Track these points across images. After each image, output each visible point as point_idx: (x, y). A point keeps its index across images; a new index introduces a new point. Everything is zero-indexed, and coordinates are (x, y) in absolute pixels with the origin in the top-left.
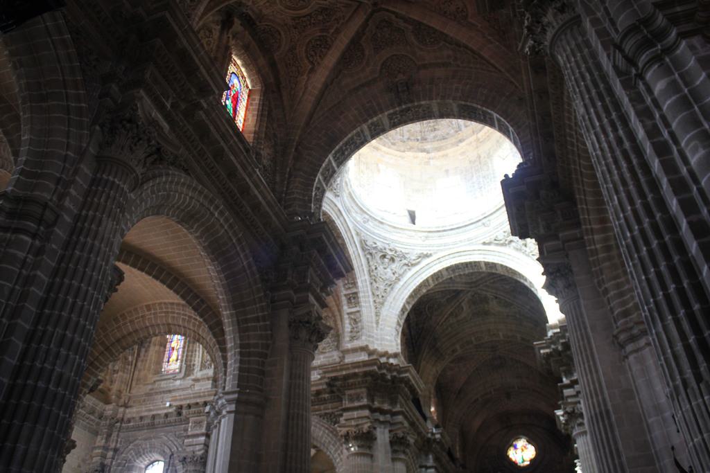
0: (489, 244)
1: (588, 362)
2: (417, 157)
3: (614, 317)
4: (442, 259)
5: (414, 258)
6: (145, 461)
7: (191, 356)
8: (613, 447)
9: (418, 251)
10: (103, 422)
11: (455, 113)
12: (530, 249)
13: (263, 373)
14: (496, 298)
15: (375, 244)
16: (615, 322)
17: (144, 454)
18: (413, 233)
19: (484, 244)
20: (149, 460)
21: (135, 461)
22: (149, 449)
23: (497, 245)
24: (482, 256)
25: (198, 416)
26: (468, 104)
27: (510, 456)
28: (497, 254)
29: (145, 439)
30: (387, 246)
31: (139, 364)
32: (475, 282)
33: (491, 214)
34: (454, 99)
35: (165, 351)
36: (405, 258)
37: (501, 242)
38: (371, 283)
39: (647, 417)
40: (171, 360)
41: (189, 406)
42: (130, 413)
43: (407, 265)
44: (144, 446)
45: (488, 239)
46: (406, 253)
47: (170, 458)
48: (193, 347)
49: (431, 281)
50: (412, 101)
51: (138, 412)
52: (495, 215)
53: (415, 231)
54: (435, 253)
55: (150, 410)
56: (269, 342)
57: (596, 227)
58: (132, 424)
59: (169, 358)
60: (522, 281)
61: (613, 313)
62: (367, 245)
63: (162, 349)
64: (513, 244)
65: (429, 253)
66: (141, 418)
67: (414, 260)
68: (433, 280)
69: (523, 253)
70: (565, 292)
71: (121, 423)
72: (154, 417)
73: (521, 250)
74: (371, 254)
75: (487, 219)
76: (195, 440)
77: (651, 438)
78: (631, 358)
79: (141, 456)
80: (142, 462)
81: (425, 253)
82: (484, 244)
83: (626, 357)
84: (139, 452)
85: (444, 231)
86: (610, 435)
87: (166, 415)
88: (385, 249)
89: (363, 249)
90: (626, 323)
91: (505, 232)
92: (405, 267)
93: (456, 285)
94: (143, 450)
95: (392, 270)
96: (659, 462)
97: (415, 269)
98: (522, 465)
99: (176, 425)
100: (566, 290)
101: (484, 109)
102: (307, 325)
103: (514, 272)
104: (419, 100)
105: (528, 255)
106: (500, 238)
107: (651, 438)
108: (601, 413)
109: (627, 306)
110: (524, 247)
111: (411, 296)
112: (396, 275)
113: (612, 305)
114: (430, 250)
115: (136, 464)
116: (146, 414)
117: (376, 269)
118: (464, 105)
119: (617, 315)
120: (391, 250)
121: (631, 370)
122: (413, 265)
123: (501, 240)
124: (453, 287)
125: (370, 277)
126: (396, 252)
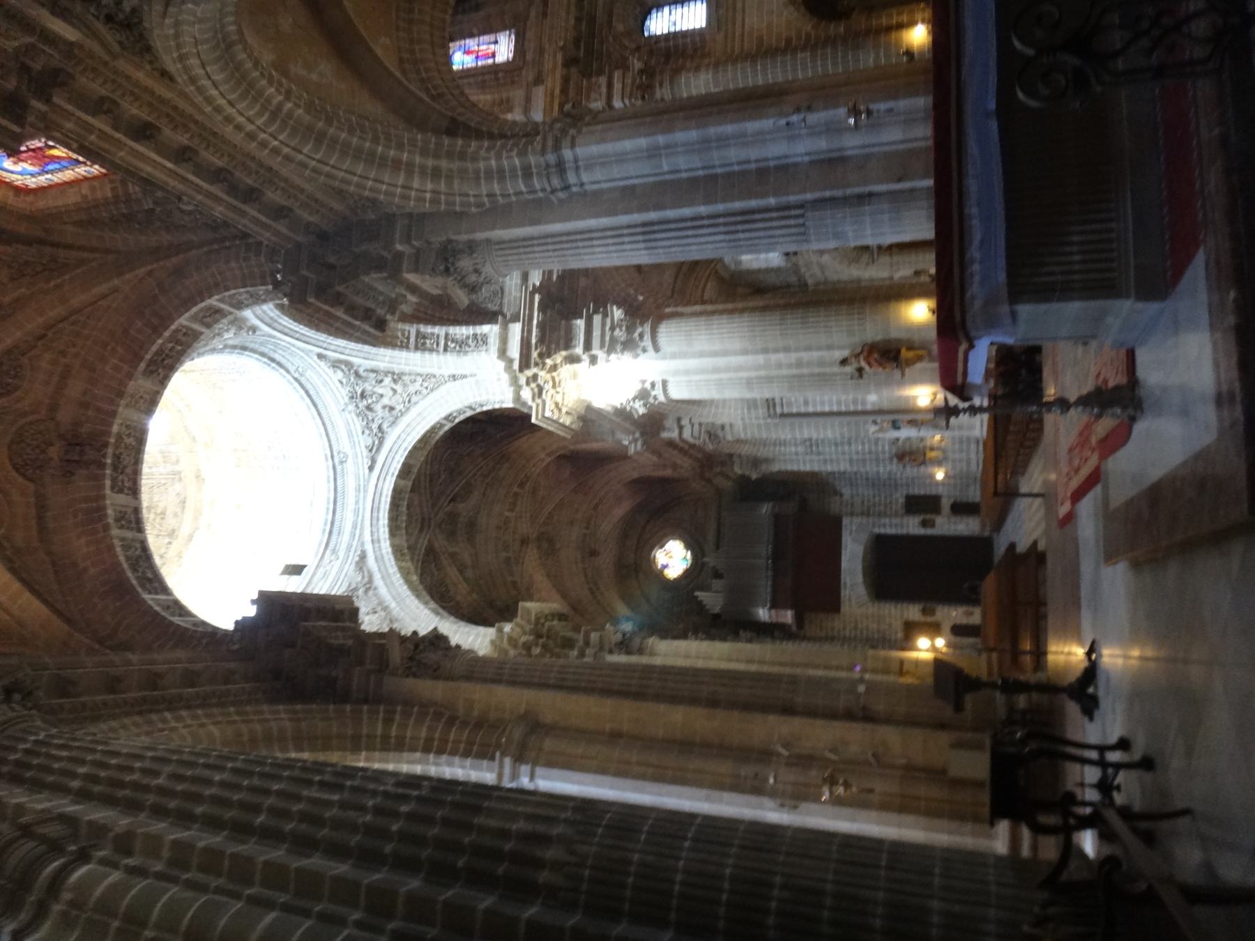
0: (373, 461)
1: (576, 241)
3: (527, 193)
8: (689, 224)
9: (350, 568)
11: (155, 388)
12: (398, 404)
13: (479, 725)
14: (453, 500)
16: (534, 192)
18: (321, 571)
19: (371, 468)
23: (378, 450)
24: (389, 477)
26: (148, 357)
27: (675, 576)
28: (392, 454)
32: (423, 519)
33: (330, 446)
34: (130, 376)
37: (377, 442)
39: (660, 171)
43: (367, 591)
46: (349, 586)
49: (404, 564)
50: (106, 445)
52: (333, 442)
53: (318, 567)
54: (363, 544)
56: (432, 710)
57: (401, 180)
60: (441, 433)
61: (521, 193)
64: (385, 426)
65: (359, 552)
67: (363, 578)
68: (403, 561)
69: (402, 415)
70: (476, 258)
73: (397, 418)
75: (335, 454)
77: (686, 171)
78: (585, 177)
81: (357, 559)
82: (371, 468)
83: (582, 185)
85: (332, 523)
86: (673, 226)
90: (539, 174)
91: (363, 432)
92: (371, 593)
93: (419, 546)
95: (368, 614)
96: (713, 167)
97: (378, 581)
98: (690, 562)
100: (475, 255)
101: (167, 334)
102: (421, 647)
103: (424, 439)
104: (108, 433)
105: (408, 409)
106: (369, 442)
107: (686, 171)
108: (644, 233)
109: (519, 168)
110: (394, 413)
111: (418, 596)
112: (379, 609)
113: (511, 192)
114: (355, 552)
118: (148, 366)
119: (525, 186)
121: (598, 182)
122: (371, 581)
123: (374, 443)
124: (420, 550)
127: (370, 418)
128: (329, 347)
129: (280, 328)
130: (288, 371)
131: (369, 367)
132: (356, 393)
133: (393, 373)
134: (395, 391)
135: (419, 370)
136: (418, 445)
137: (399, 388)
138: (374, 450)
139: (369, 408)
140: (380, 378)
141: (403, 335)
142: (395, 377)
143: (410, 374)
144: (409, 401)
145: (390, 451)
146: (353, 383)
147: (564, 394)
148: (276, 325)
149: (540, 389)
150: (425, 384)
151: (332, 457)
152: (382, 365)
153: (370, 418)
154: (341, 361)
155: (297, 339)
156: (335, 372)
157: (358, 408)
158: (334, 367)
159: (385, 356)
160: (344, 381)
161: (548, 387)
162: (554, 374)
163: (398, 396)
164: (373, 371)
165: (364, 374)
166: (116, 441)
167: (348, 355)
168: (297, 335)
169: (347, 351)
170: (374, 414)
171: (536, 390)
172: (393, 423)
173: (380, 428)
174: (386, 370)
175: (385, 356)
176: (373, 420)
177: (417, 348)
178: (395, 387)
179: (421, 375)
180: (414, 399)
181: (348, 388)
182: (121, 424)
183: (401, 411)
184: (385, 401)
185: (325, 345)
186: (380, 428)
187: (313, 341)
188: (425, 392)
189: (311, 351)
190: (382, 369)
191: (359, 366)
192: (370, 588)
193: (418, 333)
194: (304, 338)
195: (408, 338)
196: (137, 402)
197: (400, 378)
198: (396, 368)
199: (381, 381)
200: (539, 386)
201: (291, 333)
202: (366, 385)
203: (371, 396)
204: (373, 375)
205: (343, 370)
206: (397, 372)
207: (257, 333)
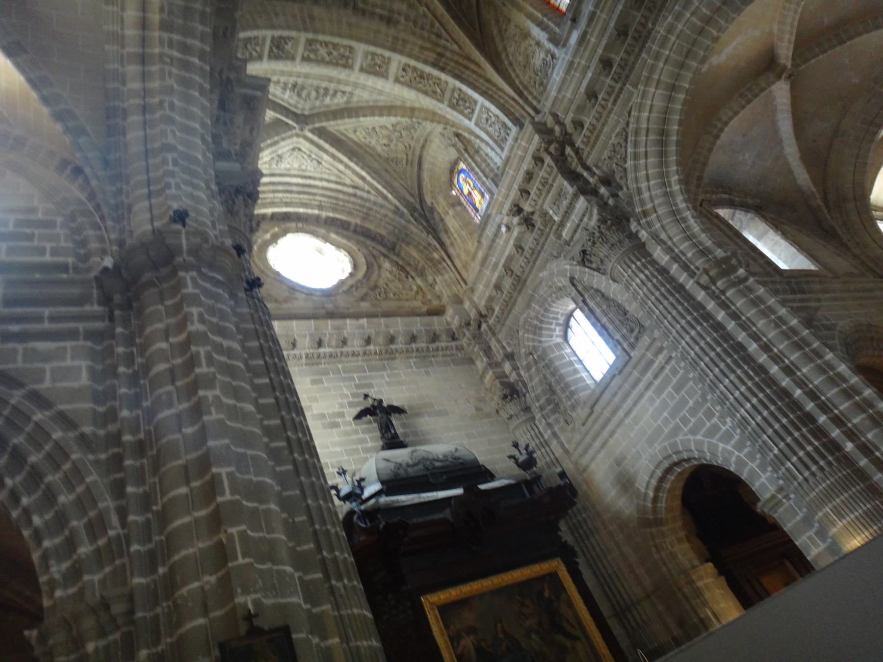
6: (554, 330)
7: (488, 165)
10: (464, 342)
17: (542, 322)
20: (558, 324)
21: (540, 342)
22: (542, 311)
25: (549, 192)
29: (528, 306)
31: (451, 251)
35: (465, 207)
40: (477, 205)
41: (525, 192)
42: (480, 298)
44: (533, 314)
47: (574, 285)
48: (481, 157)
51: (487, 286)
55: (496, 265)
58: (497, 309)
59: (474, 206)
63: (458, 208)
66: (498, 287)
71: (486, 322)
72: (508, 268)
76: (574, 217)
79: (541, 329)
80: (551, 336)
84: (535, 327)
87: (519, 247)
94: (537, 318)
99: (543, 244)
115: (545, 345)
116: (496, 275)
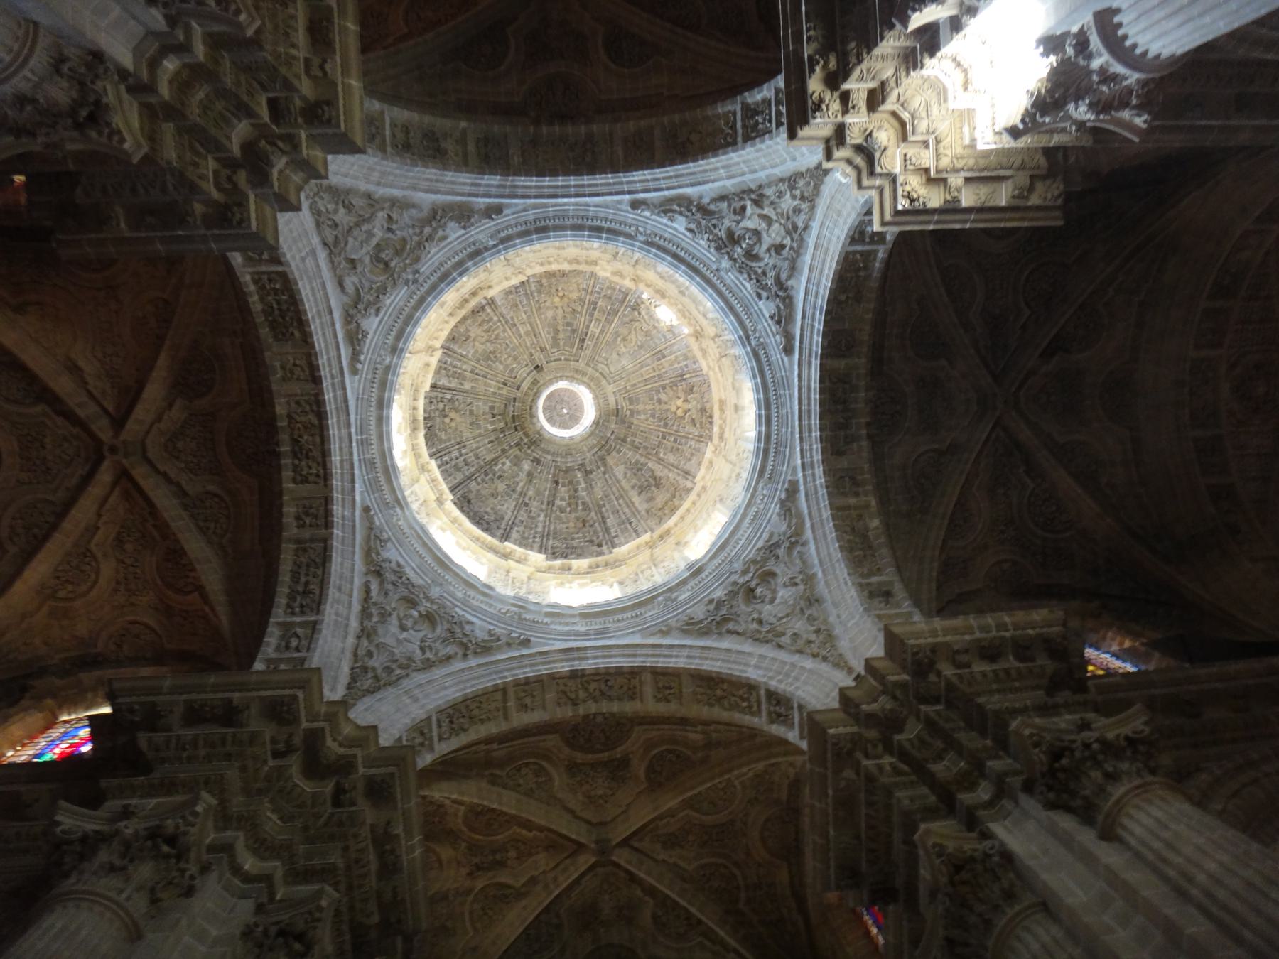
0: (789, 337)
2: (711, 462)
4: (807, 460)
5: (784, 528)
9: (775, 509)
12: (784, 238)
15: (711, 601)
19: (788, 350)
23: (790, 318)
24: (813, 360)
30: (734, 578)
36: (777, 545)
38: (780, 646)
43: (790, 550)
45: (778, 337)
46: (771, 535)
62: (701, 622)
64: (783, 276)
68: (844, 494)
74: (725, 620)
81: (783, 496)
88: (735, 583)
89: (704, 633)
91: (759, 296)
105: (802, 240)
110: (785, 252)
114: (784, 483)
117: (760, 622)
120: (745, 572)
122: (799, 532)
123: (778, 307)
125: (767, 642)
126: (754, 562)
127: (760, 271)
128: (633, 187)
129: (533, 192)
130: (628, 236)
131: (713, 195)
132: (721, 239)
133: (751, 191)
134: (765, 218)
135: (779, 172)
136: (843, 298)
137: (767, 211)
138: (783, 319)
139: (751, 255)
140: (737, 205)
141: (727, 123)
142: (753, 196)
143: (769, 185)
144: (795, 228)
145: (803, 317)
146: (707, 227)
147: (938, 142)
148: (520, 191)
149: (867, 152)
150: (798, 192)
151: (748, 337)
152: (729, 185)
153: (760, 271)
154: (670, 200)
155: (577, 196)
156: (671, 220)
157: (735, 260)
158: (665, 212)
159: (716, 169)
160: (693, 226)
161: (885, 136)
162: (890, 105)
163: (776, 226)
164: (722, 198)
165: (712, 207)
166: (290, 423)
167: (668, 189)
168: (573, 191)
169: (663, 184)
170: (762, 264)
171: (859, 160)
172: (793, 269)
173: (778, 282)
174: (738, 191)
175: (716, 169)
176: (764, 274)
177: (748, 138)
178: (765, 212)
179: (782, 180)
180: (800, 225)
181: (706, 236)
182: (288, 403)
183: (792, 248)
184: (767, 241)
185: (626, 188)
186: (778, 282)
187: (605, 189)
188: (805, 206)
189: (619, 202)
190: (733, 191)
191: (701, 197)
192: (797, 542)
193: (746, 107)
194: (587, 190)
195: (733, 127)
196: (292, 372)
197: (762, 196)
198: (750, 180)
199: (743, 208)
200: (859, 149)
201: (559, 191)
202: (727, 223)
203: (743, 237)
204: (724, 205)
205: (681, 213)
206: (753, 187)
207: (505, 212)
